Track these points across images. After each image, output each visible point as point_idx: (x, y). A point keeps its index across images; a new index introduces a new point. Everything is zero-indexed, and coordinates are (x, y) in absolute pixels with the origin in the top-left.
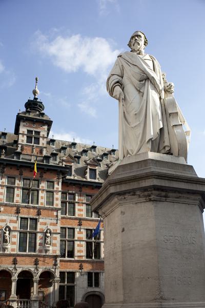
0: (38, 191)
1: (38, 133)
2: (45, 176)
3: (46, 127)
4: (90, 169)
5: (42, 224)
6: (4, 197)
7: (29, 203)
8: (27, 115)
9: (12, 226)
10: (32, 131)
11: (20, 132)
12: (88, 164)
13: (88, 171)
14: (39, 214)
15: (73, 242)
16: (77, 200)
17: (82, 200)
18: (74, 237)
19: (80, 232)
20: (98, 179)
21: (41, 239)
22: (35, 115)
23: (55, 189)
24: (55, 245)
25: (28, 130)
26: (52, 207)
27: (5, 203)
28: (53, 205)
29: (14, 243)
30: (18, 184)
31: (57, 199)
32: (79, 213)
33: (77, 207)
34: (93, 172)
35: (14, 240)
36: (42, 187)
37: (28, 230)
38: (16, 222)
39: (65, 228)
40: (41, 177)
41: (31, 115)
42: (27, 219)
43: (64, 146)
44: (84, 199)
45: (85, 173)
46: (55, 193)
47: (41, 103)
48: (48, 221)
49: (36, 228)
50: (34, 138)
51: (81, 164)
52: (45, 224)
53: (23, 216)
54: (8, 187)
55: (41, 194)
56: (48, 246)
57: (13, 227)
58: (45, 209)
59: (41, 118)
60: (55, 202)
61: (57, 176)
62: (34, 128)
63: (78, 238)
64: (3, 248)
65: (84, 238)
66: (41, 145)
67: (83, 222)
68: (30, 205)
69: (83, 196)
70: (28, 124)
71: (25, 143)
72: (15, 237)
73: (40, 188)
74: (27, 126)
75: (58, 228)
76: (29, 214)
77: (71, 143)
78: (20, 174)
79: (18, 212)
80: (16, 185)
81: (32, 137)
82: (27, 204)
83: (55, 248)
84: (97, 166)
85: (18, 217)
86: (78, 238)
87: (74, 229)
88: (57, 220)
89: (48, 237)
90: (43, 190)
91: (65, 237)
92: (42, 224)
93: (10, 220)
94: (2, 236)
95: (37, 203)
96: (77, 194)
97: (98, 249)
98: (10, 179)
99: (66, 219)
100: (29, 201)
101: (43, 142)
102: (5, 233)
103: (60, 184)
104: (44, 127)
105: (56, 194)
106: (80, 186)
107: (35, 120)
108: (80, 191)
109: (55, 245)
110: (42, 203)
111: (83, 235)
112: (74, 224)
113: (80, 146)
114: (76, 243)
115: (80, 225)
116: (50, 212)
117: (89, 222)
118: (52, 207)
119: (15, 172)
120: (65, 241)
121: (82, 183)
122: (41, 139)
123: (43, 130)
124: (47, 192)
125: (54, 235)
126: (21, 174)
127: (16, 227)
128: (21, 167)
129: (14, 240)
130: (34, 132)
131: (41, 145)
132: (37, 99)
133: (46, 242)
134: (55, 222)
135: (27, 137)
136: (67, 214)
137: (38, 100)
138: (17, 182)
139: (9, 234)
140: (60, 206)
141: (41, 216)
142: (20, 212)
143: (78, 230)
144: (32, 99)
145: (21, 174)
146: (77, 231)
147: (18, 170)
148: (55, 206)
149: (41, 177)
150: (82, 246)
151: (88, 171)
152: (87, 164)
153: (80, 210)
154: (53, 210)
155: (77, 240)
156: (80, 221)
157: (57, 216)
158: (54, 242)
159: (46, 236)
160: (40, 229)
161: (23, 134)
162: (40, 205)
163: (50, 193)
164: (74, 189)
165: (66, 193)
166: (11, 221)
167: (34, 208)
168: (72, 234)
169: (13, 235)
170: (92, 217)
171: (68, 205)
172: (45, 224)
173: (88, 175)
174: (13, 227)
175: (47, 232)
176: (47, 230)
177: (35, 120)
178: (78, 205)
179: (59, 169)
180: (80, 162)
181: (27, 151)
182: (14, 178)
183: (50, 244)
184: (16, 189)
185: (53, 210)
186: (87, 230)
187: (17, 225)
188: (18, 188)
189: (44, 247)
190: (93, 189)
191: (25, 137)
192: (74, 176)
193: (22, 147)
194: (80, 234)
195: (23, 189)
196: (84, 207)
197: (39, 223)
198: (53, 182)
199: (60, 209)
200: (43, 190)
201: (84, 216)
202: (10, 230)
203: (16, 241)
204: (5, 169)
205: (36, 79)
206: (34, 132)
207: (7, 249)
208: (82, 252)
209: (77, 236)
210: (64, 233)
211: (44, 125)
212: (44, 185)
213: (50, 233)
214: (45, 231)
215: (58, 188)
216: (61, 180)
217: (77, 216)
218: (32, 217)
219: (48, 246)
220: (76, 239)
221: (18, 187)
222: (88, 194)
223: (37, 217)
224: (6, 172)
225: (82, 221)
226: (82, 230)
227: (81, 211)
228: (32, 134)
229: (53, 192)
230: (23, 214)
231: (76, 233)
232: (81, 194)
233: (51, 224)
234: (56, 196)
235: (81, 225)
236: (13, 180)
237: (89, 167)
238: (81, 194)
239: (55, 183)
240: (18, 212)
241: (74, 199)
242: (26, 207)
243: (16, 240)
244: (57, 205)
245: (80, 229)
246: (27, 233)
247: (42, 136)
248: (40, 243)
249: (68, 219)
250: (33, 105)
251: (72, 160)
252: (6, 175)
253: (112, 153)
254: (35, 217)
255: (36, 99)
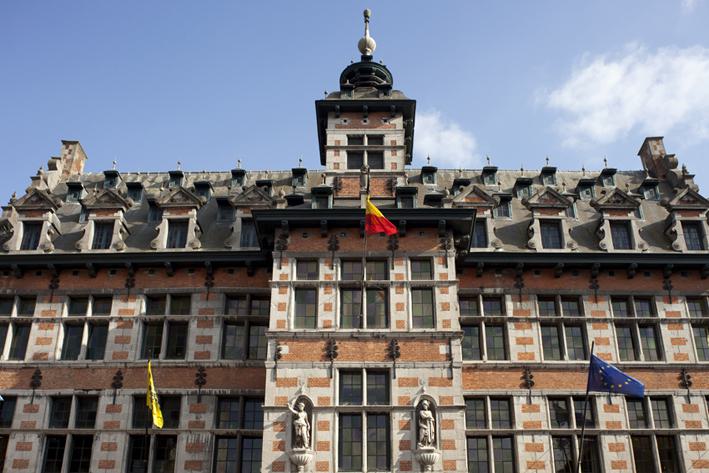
0: (386, 290)
1: (379, 139)
2: (402, 244)
3: (399, 122)
4: (542, 221)
5: (403, 383)
6: (289, 314)
7: (361, 326)
8: (344, 97)
9: (314, 395)
10: (360, 139)
11: (329, 144)
12: (532, 208)
13: (536, 225)
14: (393, 354)
15: (512, 437)
16: (510, 314)
17: (529, 312)
18: (511, 422)
19: (530, 407)
20: (570, 246)
21: (406, 427)
22: (366, 96)
23: (437, 278)
24: (449, 445)
25: (349, 137)
26: (433, 330)
27: (293, 328)
28: (434, 324)
29: (323, 446)
30: (326, 276)
31: (446, 307)
32: (521, 348)
33: (513, 333)
34: (552, 228)
35: (323, 436)
36: (399, 276)
37: (365, 403)
38: (324, 383)
39: (482, 398)
40: (393, 247)
41: (356, 96)
42: (358, 372)
43: (462, 177)
44: (533, 309)
45: (530, 233)
46: (437, 291)
47: (384, 67)
48: (423, 373)
49: (387, 398)
50: (369, 153)
51: (516, 214)
52: (414, 382)
53: (346, 364)
54: (298, 289)
55: (395, 297)
56: (426, 448)
57: (320, 399)
58: (409, 338)
59: (382, 97)
60: (441, 315)
61: (439, 240)
62: (365, 127)
63: (525, 424)
64: (292, 463)
65: (544, 423)
66: (388, 168)
67: (537, 376)
68: (365, 329)
69: (528, 299)
70: (349, 121)
71: (344, 168)
72: (324, 426)
73: (392, 278)
74: (345, 127)
75: (456, 393)
76: (362, 358)
77: (480, 173)
78: (330, 249)
79: (330, 354)
80: (322, 278)
81: (361, 154)
82: (355, 330)
83: (450, 454)
84: (560, 210)
85: (331, 368)
86: (525, 424)
87: (508, 399)
88: (451, 367)
89: (425, 420)
90: (402, 285)
91: (486, 426)
92: (403, 383)
93: (310, 380)
94: (289, 425)
95: (387, 324)
96: (508, 297)
97: (593, 458)
98: (304, 265)
99: (481, 370)
100: (362, 318)
101: (392, 160)
102: (296, 417)
103: (452, 262)
104: (393, 122)
105: (442, 293)
106: (518, 269)
107: (366, 107)
108: (519, 286)
109: (449, 445)
110: (400, 323)
111: (543, 415)
112: (509, 384)
113: (508, 176)
114: (522, 441)
115: (528, 384)
116: (426, 346)
117: (554, 375)
118: (433, 330)
119: (315, 244)
120: (486, 437)
121: (521, 261)
122: (387, 154)
123: (392, 131)
124: (413, 289)
125: (446, 416)
126: (334, 247)
127: (328, 399)
128: (333, 226)
129: (323, 436)
130: (366, 139)
131: (388, 168)
132: (371, 57)
133: (422, 437)
134: (445, 373)
135: (349, 153)
136: (485, 357)
137: (373, 60)
138: (324, 270)
139: (309, 419)
140: (456, 327)
141: (399, 361)
142: (335, 355)
143: (523, 400)
144: (358, 59)
145: (334, 247)
146: (519, 403)
147: (324, 236)
148: (440, 327)
149: (393, 247)
150: (539, 448)
151: (536, 225)
152: (532, 208)
153: (520, 341)
154: (433, 339)
155: (522, 433)
156: (527, 374)
157: (449, 357)
158: (445, 434)
159: (420, 420)
160: (400, 399)
161: (337, 148)
162: (394, 328)
163: (424, 292)
164: (498, 283)
165: (475, 298)
166: (314, 382)
167: (377, 338)
168: (504, 414)
169: (320, 423)
170: (562, 358)
171: (482, 329)
172: (414, 382)
173: (537, 241)
174: (320, 399)
175: (421, 407)
176: (421, 402)
177: (366, 107)
178: (517, 328)
179: (443, 220)
180: (511, 210)
181: (350, 188)
182: (316, 261)
183: (435, 443)
184: (321, 291)
185: (433, 339)
186: (551, 398)
187: (332, 393)
188: (327, 285)
189: (417, 451)
190: (557, 277)
191: (344, 154)
192: (494, 244)
193: (335, 180)
194: (532, 414)
195: (343, 288)
196: (535, 332)
197: (394, 383)
198: (429, 260)
199: (455, 335)
200: (402, 285)
201: (539, 358)
202: (309, 409)
203: (330, 439)
204: (289, 240)
205: (366, 16)
206: (366, 139)
207: (304, 464)
208: (543, 467)
209: (521, 418)
210: (480, 413)
211: (393, 117)
212: (401, 270)
213: (432, 408)
214: (416, 404)
215: (446, 275)
216: (452, 251)
217: (514, 359)
218: (372, 364)
219: (426, 448)
220: (519, 427)
221: (327, 285)
222: (543, 292)
223: (390, 364)
224: (291, 247)
225: (533, 373)
226: (535, 401)
227: (526, 342)
228: (362, 143)
229: (430, 289)
230: (348, 359)
231: (517, 409)
232: (520, 295)
233: (432, 382)
234: (440, 298)
235: (532, 384)
236: (312, 266)
237: (537, 215)
238: (520, 295)
239: (436, 260)
240: (330, 354)
241: (503, 310)
242: (352, 338)
243: (330, 435)
244: (447, 323)
245: (529, 397)
246: (360, 415)
247: (389, 144)
248: (401, 442)
249: (488, 369)
250: (362, 73)
251: (484, 203)
252: (291, 255)
253: (605, 181)
254: (382, 365)
255: (366, 59)
